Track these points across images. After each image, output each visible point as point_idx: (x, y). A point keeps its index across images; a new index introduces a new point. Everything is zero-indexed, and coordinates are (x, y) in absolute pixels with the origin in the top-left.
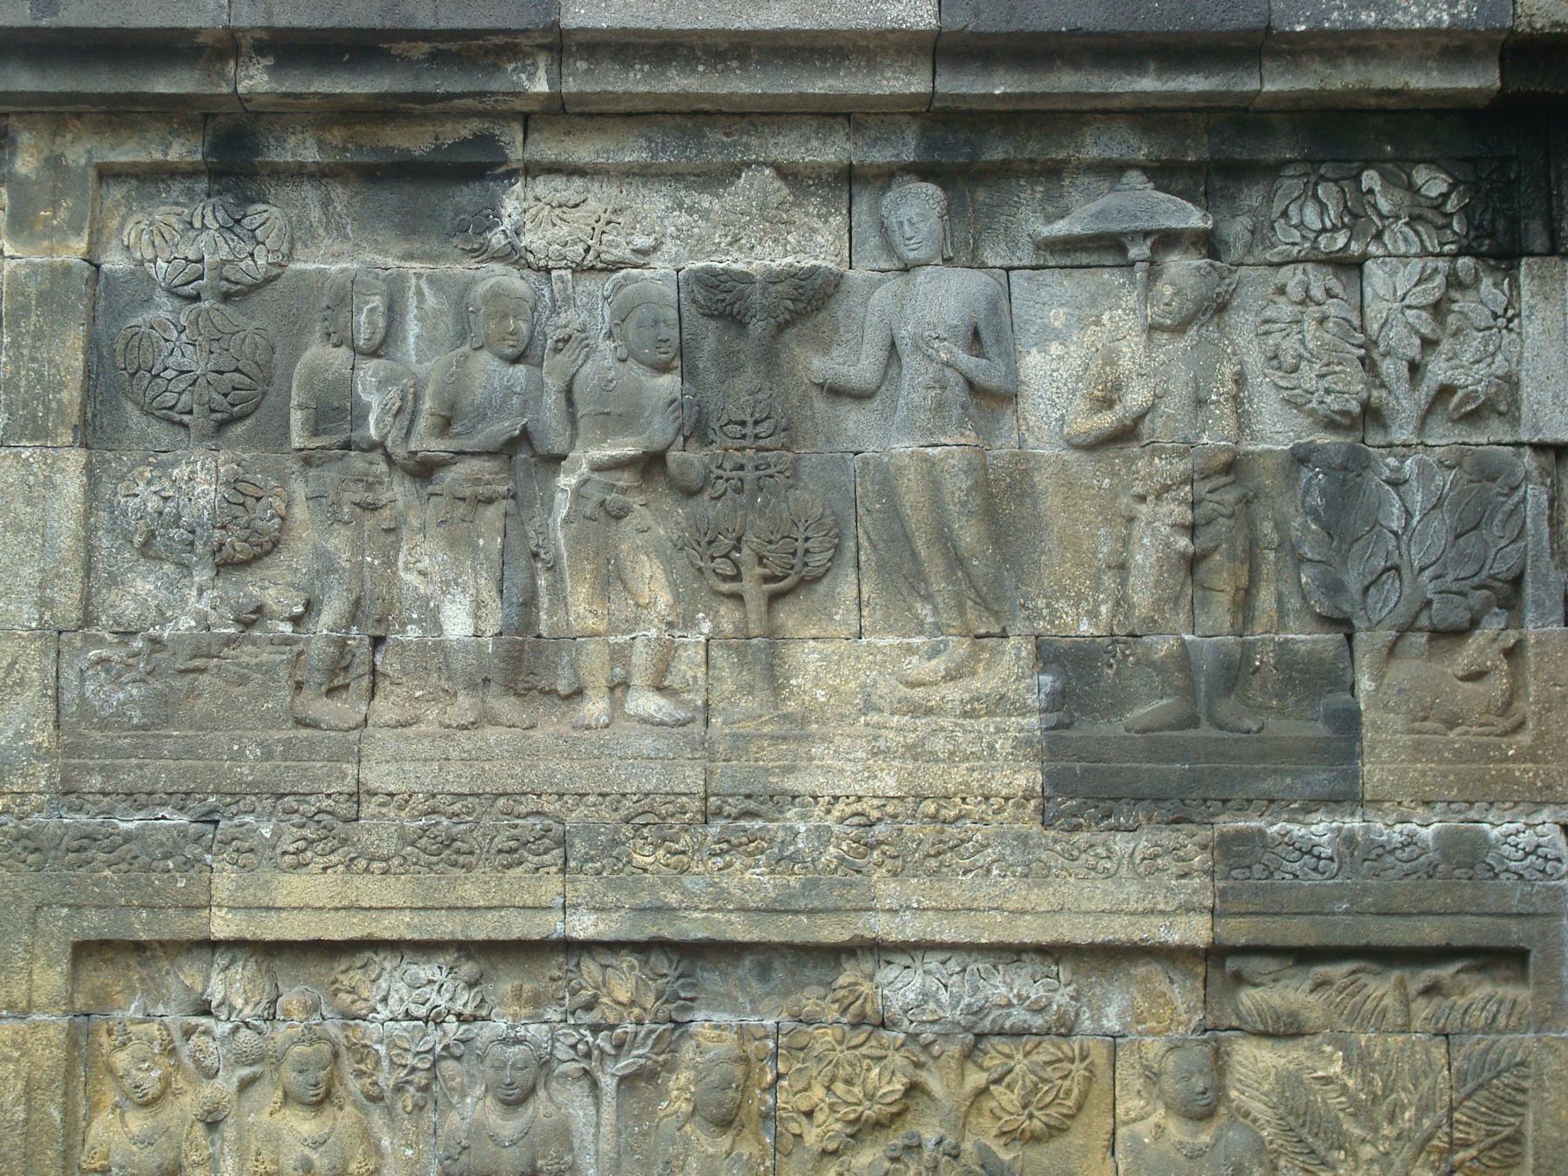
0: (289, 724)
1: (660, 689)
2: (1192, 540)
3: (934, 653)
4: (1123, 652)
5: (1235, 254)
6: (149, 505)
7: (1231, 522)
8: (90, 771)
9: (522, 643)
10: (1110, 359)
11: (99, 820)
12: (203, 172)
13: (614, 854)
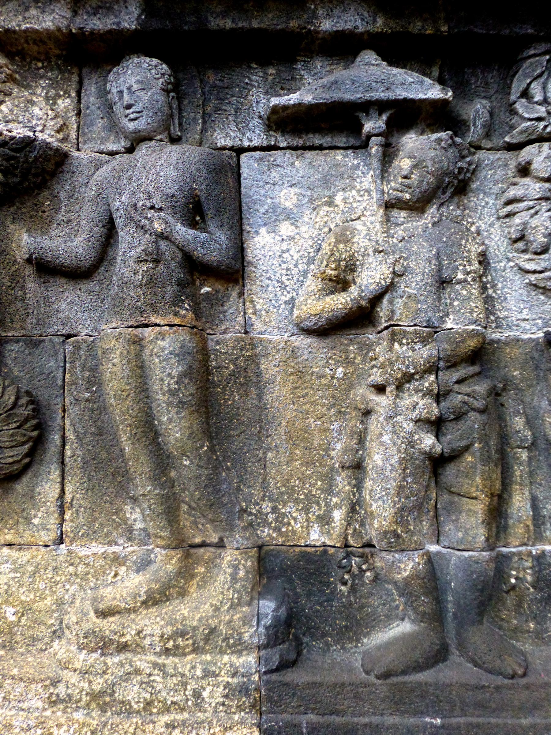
2: (437, 437)
4: (360, 568)
7: (484, 417)
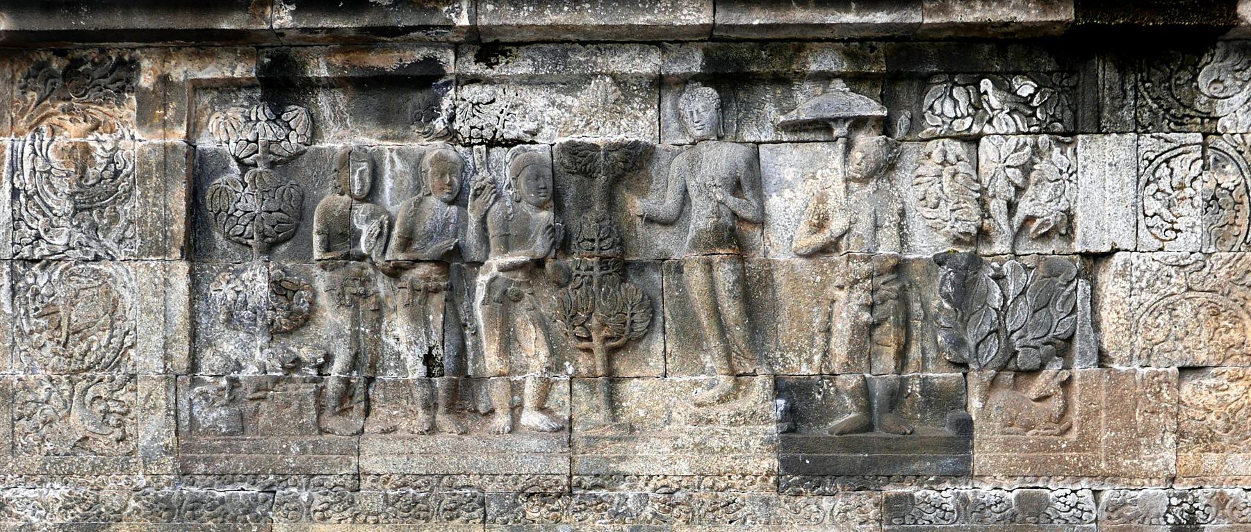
0: (317, 432)
1: (541, 409)
2: (871, 314)
3: (711, 386)
5: (900, 132)
6: (228, 296)
7: (896, 302)
8: (198, 461)
9: (457, 381)
10: (822, 200)
11: (204, 491)
12: (258, 86)
13: (515, 511)
